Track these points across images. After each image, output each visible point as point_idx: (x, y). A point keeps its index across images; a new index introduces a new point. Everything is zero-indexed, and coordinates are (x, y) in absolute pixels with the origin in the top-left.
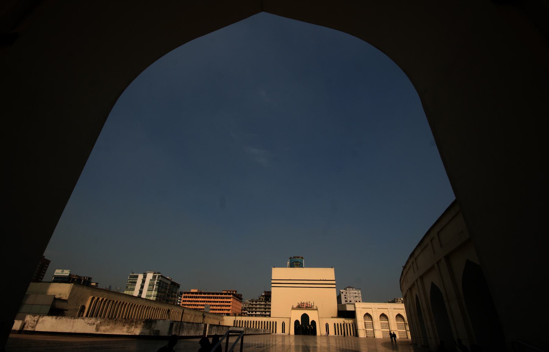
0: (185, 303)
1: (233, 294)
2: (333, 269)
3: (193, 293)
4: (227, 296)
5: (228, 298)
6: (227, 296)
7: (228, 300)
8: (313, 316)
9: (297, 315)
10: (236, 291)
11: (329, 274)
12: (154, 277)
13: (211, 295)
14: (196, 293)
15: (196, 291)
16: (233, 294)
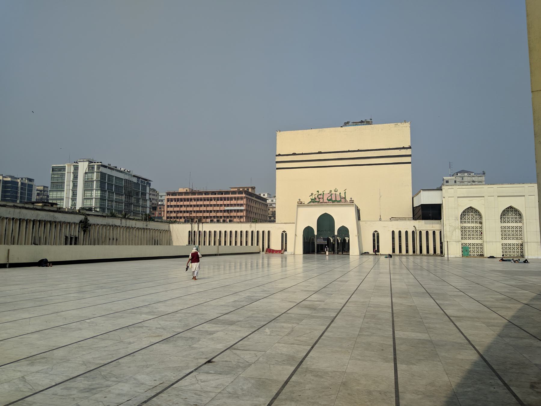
0: (171, 209)
1: (247, 193)
2: (408, 125)
3: (181, 194)
4: (237, 195)
5: (238, 199)
6: (237, 195)
7: (239, 202)
8: (343, 217)
9: (310, 218)
10: (253, 188)
11: (398, 135)
12: (91, 168)
13: (210, 196)
14: (186, 193)
15: (185, 191)
16: (247, 193)
